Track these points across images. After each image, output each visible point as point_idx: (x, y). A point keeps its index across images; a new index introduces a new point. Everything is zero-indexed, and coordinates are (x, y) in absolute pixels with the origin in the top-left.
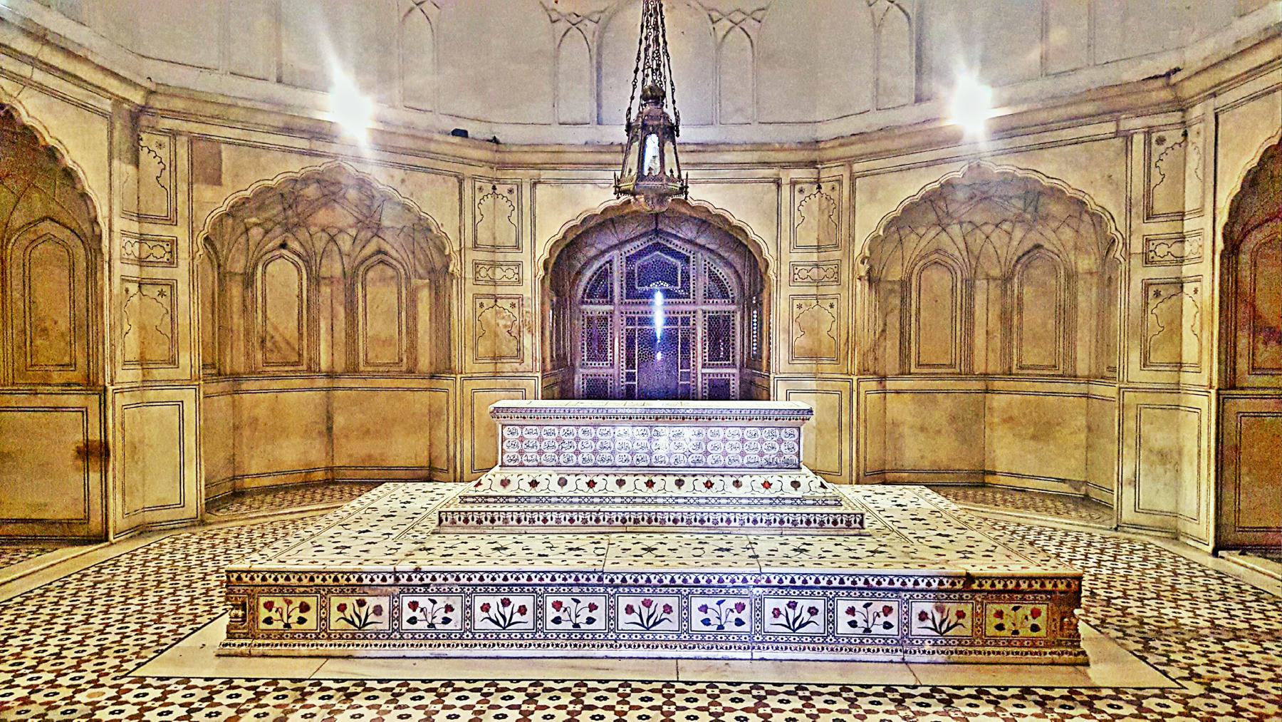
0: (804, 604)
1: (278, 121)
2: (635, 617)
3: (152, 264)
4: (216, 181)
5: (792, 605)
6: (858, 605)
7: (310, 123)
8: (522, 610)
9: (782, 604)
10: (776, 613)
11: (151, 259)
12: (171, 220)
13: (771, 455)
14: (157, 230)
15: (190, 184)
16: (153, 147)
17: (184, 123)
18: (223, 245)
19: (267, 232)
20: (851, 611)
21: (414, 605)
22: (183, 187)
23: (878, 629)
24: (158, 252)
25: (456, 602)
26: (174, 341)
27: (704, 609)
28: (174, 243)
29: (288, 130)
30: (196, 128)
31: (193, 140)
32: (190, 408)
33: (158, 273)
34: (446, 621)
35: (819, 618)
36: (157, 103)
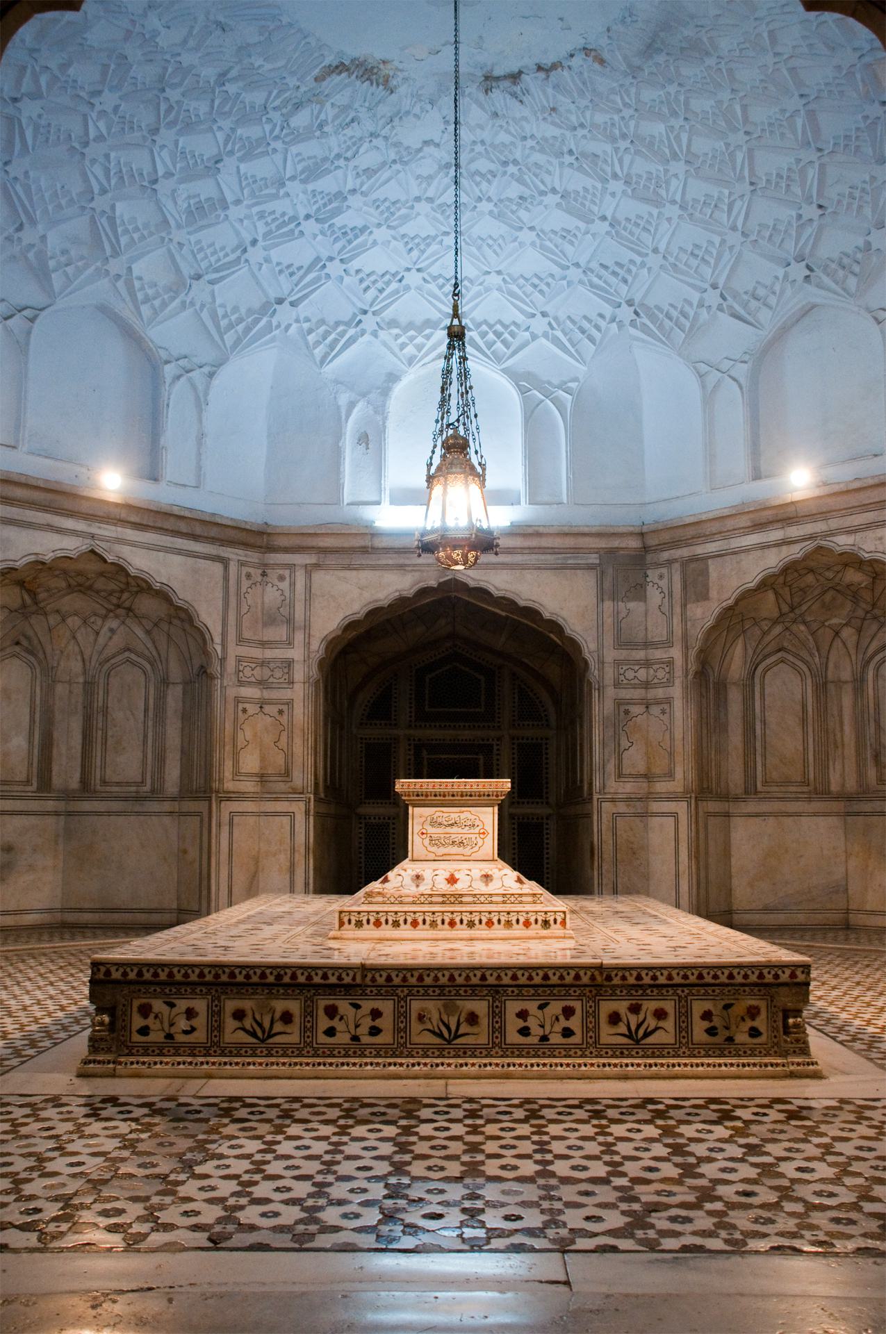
1: (744, 522)
3: (655, 686)
4: (704, 596)
7: (773, 512)
11: (656, 681)
12: (668, 644)
14: (658, 654)
15: (684, 606)
16: (656, 580)
17: (685, 550)
18: (812, 655)
19: (859, 631)
22: (678, 610)
24: (661, 674)
26: (671, 754)
28: (670, 663)
29: (758, 526)
30: (684, 552)
31: (686, 563)
32: (683, 818)
33: (660, 693)
36: (652, 541)
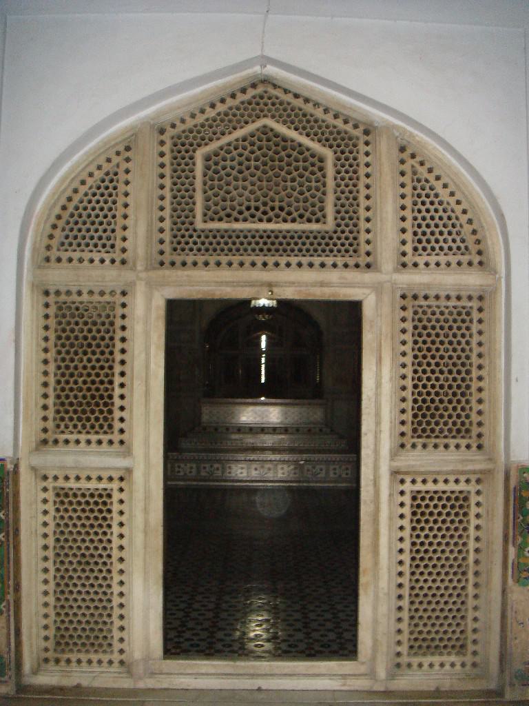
0: (318, 467)
2: (257, 472)
5: (314, 468)
6: (337, 467)
8: (218, 469)
9: (310, 467)
10: (308, 470)
13: (312, 419)
20: (335, 469)
21: (179, 467)
23: (344, 476)
25: (194, 466)
27: (282, 468)
34: (191, 472)
35: (324, 471)
